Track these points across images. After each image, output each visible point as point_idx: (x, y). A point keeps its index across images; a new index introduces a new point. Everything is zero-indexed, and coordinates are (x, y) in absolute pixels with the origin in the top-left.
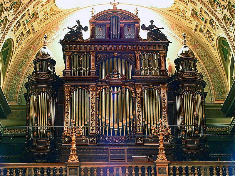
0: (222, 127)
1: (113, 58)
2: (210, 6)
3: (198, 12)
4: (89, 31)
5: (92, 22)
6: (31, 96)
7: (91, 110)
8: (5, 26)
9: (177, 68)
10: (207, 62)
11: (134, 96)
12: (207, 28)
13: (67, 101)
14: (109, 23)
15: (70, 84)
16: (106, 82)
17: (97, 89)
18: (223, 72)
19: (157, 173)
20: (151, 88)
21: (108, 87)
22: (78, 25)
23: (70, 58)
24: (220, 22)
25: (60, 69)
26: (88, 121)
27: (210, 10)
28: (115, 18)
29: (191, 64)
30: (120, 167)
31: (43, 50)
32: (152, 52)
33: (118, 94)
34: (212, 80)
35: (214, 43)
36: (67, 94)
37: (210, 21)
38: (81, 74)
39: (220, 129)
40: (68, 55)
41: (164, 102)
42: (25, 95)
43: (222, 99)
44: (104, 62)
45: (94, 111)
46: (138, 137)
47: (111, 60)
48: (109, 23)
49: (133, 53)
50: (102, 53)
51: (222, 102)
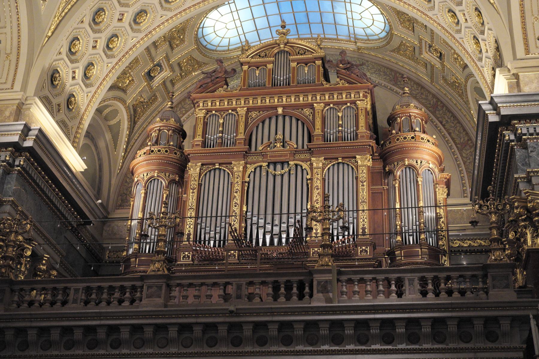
13: (193, 190)
14: (269, 62)
16: (263, 155)
17: (245, 168)
19: (315, 291)
21: (265, 164)
28: (283, 54)
30: (244, 283)
33: (282, 176)
34: (465, 159)
36: (194, 178)
41: (363, 185)
45: (238, 204)
47: (273, 121)
48: (269, 62)
49: (311, 106)
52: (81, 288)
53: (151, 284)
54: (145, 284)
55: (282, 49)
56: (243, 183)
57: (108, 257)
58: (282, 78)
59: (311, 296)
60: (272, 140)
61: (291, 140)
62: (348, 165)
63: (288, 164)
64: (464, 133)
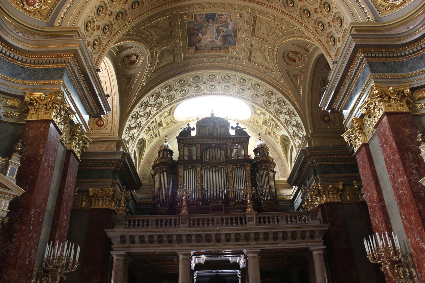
1: (212, 148)
2: (275, 114)
3: (267, 120)
4: (195, 131)
5: (197, 125)
7: (197, 182)
8: (140, 128)
9: (256, 155)
11: (227, 172)
17: (201, 169)
19: (247, 221)
21: (209, 167)
24: (282, 124)
25: (176, 156)
26: (195, 190)
27: (276, 117)
31: (165, 144)
32: (239, 144)
33: (216, 172)
38: (190, 158)
39: (285, 197)
42: (152, 175)
43: (285, 177)
46: (231, 201)
50: (204, 144)
51: (286, 179)
59: (246, 223)
62: (241, 168)
63: (218, 167)
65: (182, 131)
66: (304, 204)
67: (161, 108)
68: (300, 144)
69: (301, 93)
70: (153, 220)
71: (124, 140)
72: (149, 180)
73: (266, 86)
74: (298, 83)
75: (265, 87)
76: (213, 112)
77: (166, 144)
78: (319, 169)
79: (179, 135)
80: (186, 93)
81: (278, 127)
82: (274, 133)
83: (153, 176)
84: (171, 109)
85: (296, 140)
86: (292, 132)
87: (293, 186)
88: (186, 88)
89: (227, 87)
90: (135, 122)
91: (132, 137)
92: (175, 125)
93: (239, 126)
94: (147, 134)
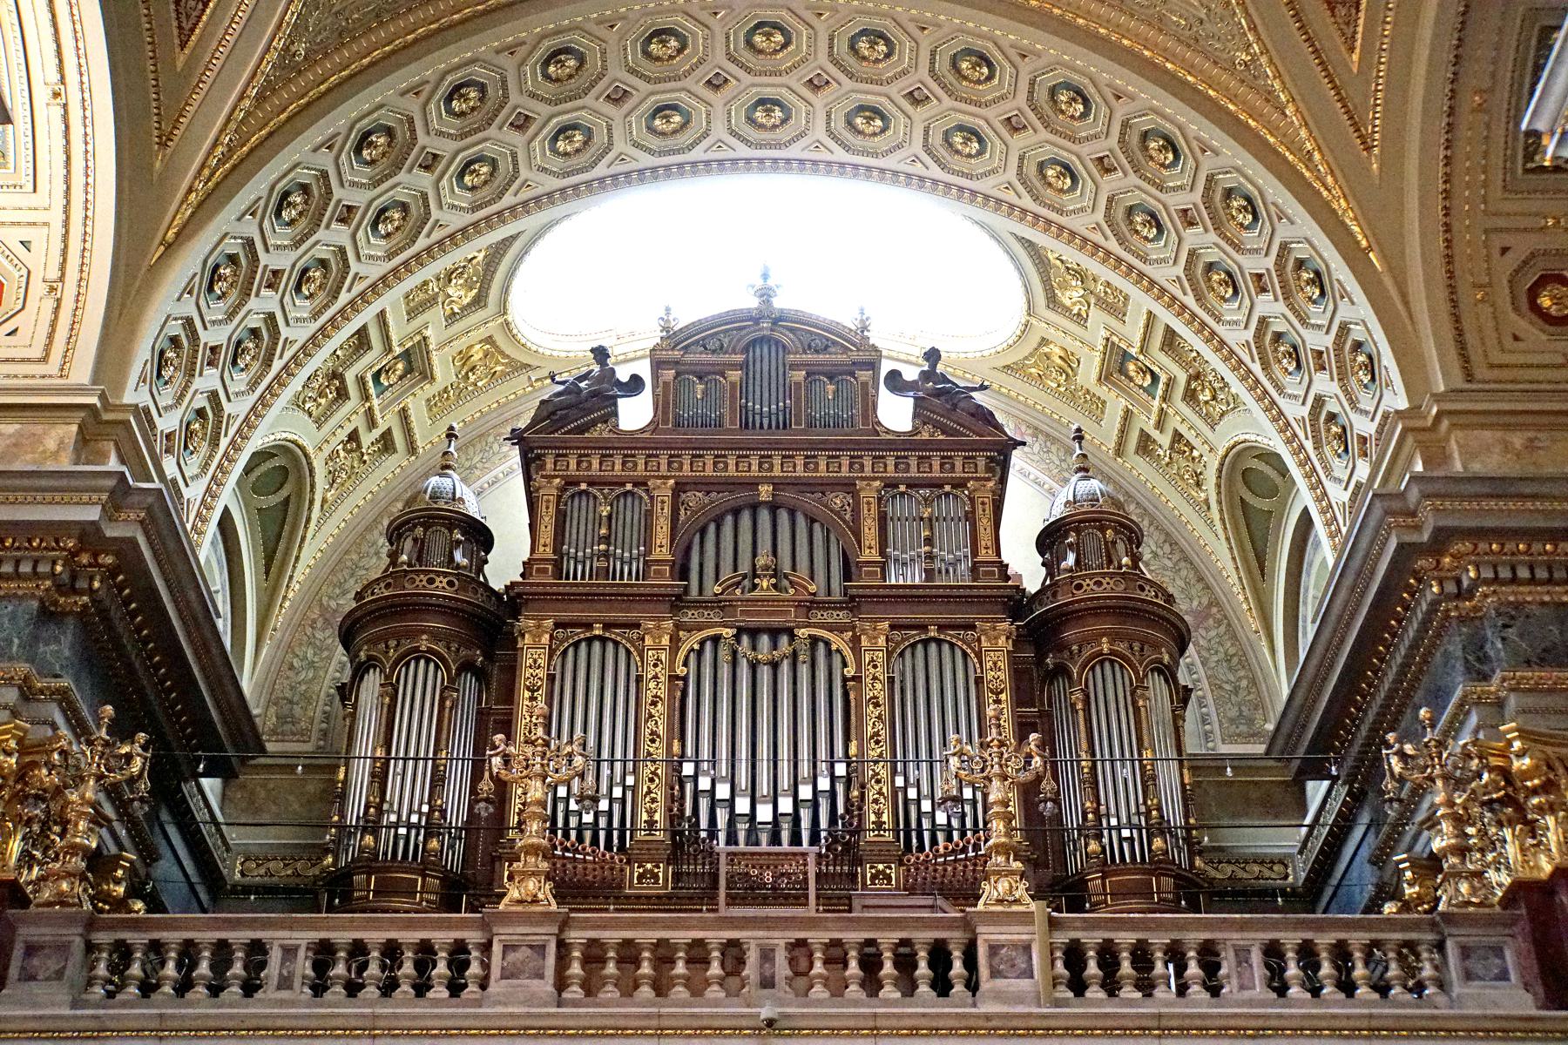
0: (1260, 860)
1: (754, 508)
2: (1190, 301)
3: (1133, 351)
4: (646, 398)
5: (657, 366)
6: (362, 679)
8: (268, 363)
10: (1177, 578)
12: (1174, 423)
13: (533, 691)
14: (734, 366)
15: (550, 617)
16: (722, 608)
17: (675, 642)
18: (1254, 624)
20: (933, 639)
21: (728, 632)
22: (596, 368)
23: (558, 505)
26: (630, 780)
29: (1114, 543)
30: (782, 943)
31: (434, 481)
33: (775, 666)
34: (1204, 653)
35: (1202, 495)
36: (535, 661)
37: (1188, 383)
40: (549, 492)
41: (998, 702)
43: (1253, 736)
44: (712, 528)
45: (659, 736)
46: (873, 863)
48: (734, 366)
49: (848, 486)
50: (706, 485)
51: (1260, 749)
52: (304, 944)
53: (516, 937)
54: (495, 940)
55: (766, 333)
56: (673, 678)
57: (243, 874)
58: (766, 409)
59: (972, 986)
60: (745, 568)
61: (794, 568)
63: (792, 636)
64: (1200, 586)
65: (559, 394)
66: (1396, 895)
67: (422, 243)
68: (1358, 486)
69: (1376, 124)
70: (296, 949)
71: (144, 415)
72: (324, 734)
73: (1132, 98)
74: (1355, 57)
75: (1122, 110)
76: (771, 282)
77: (446, 483)
78: (1511, 633)
79: (535, 421)
80: (592, 150)
81: (1205, 396)
82: (1177, 436)
83: (346, 692)
84: (496, 253)
85: (1328, 470)
86: (1305, 411)
87: (1316, 790)
88: (592, 109)
89: (869, 119)
90: (231, 315)
91: (210, 417)
92: (519, 383)
93: (940, 368)
94: (319, 423)
